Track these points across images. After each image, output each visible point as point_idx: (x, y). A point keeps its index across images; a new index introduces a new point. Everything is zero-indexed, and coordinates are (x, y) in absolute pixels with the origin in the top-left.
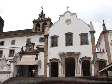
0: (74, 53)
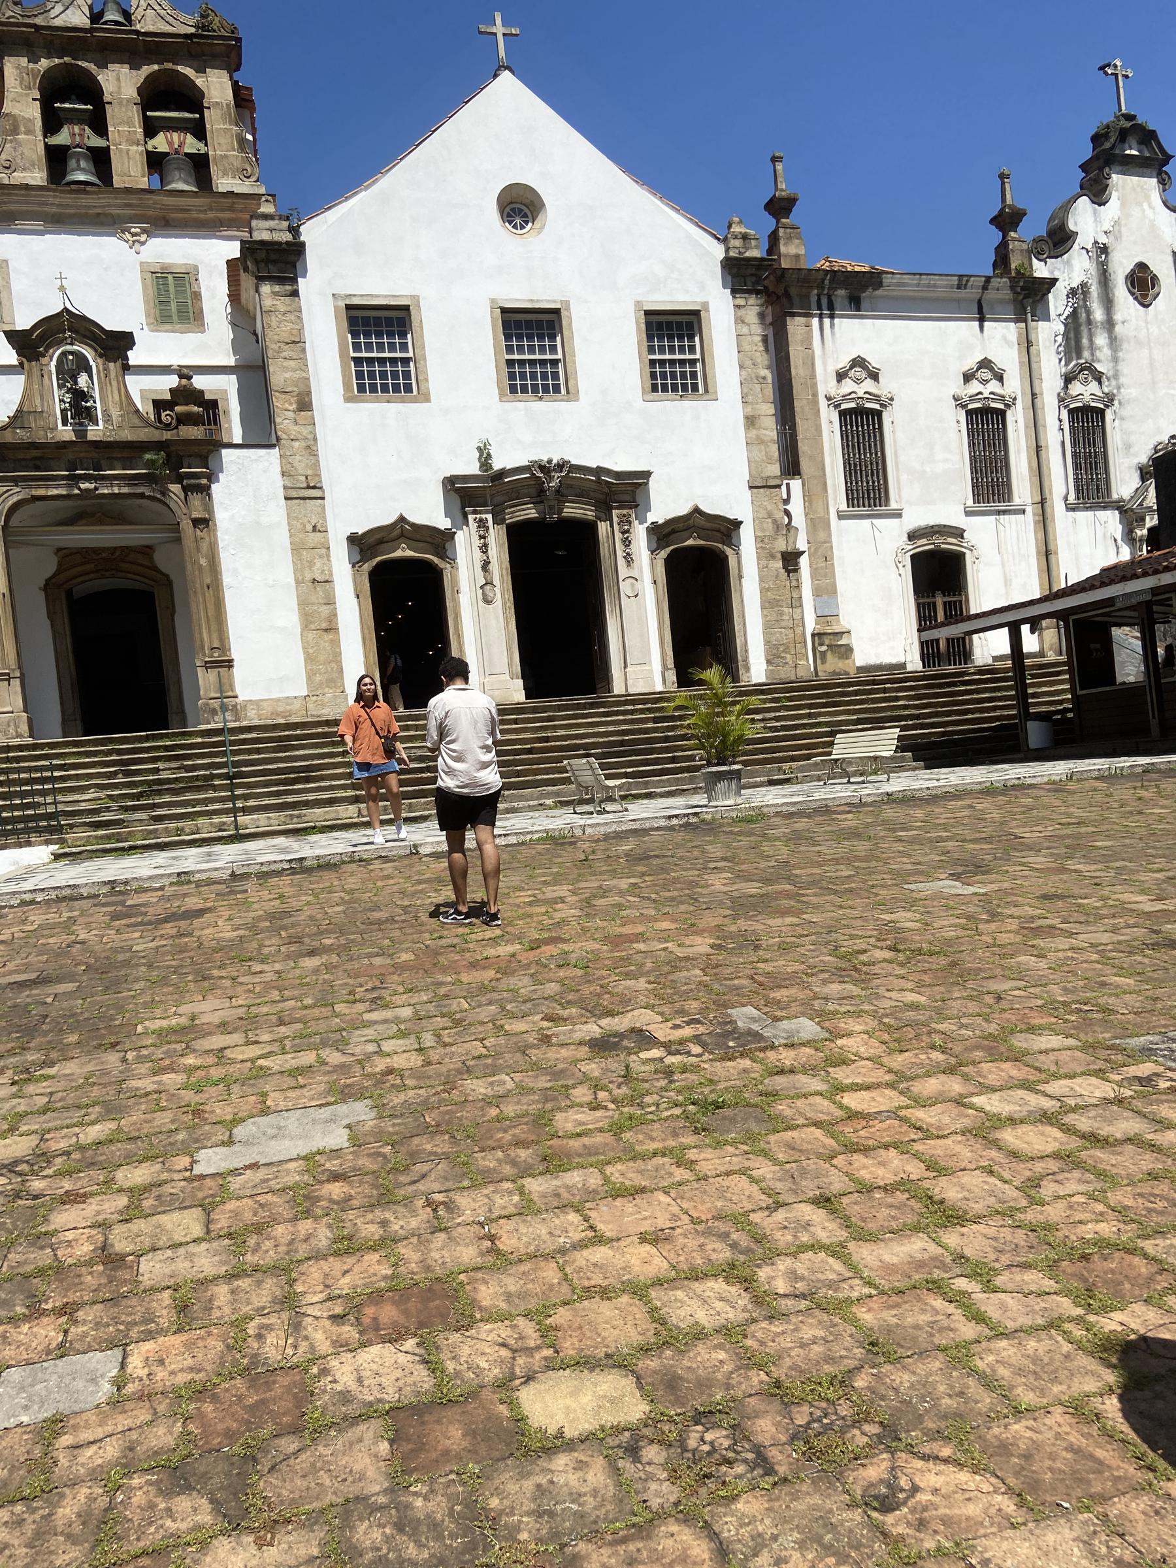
0: (599, 471)
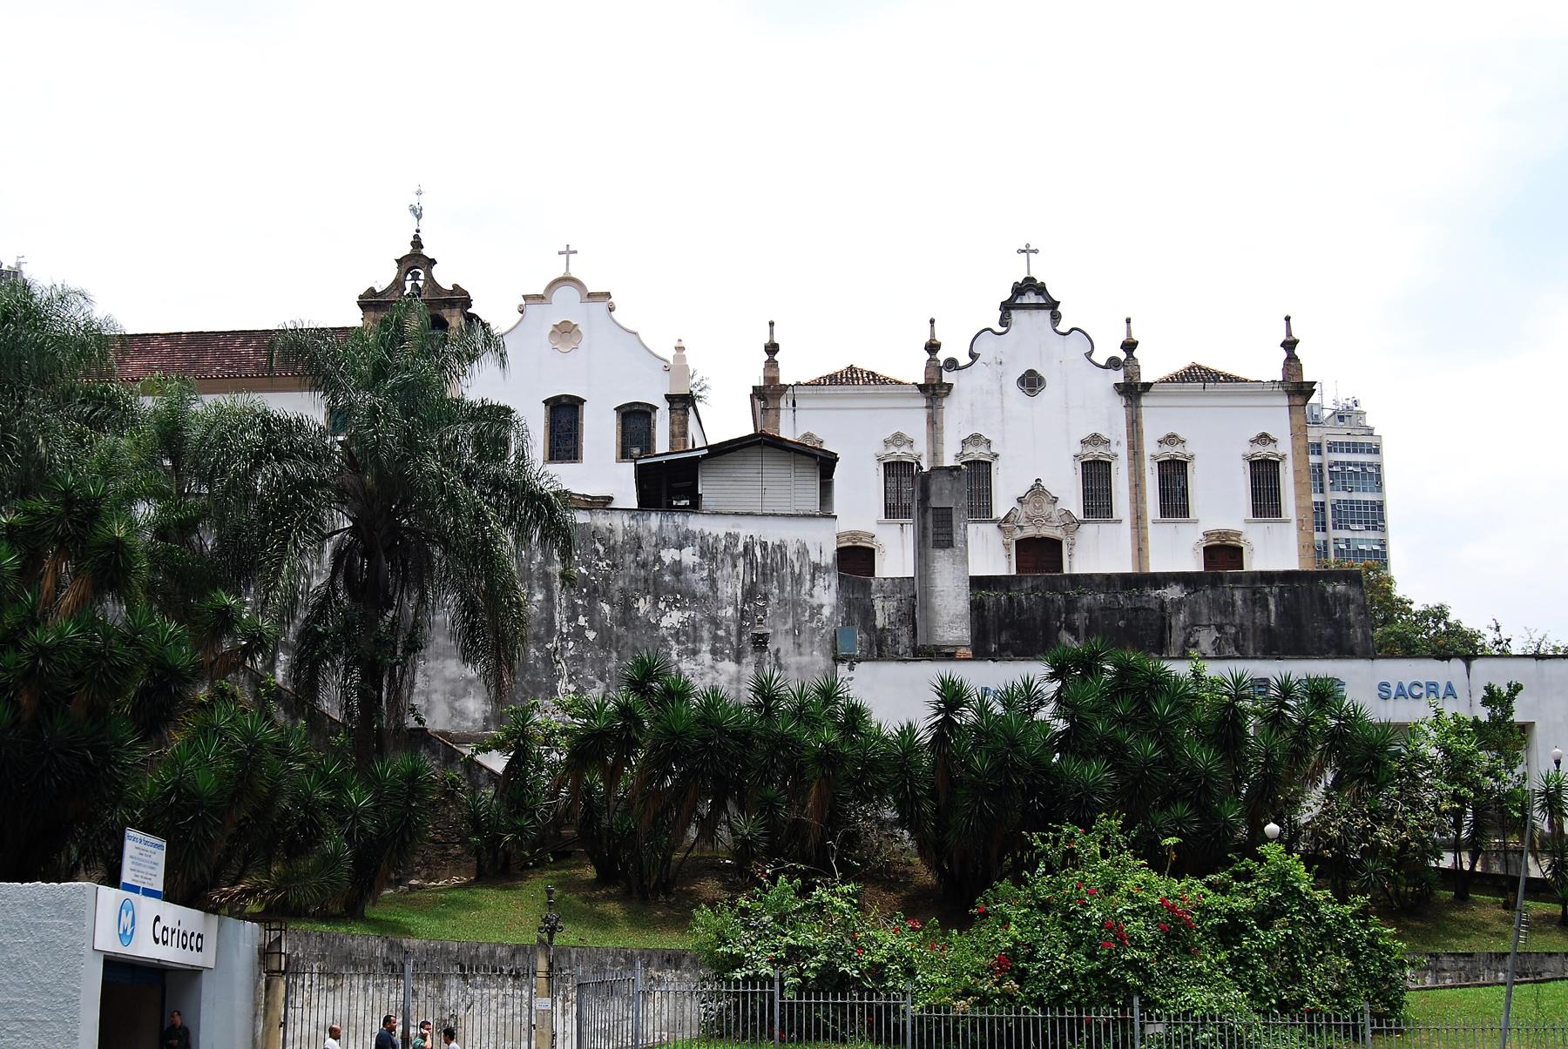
0: (584, 496)
